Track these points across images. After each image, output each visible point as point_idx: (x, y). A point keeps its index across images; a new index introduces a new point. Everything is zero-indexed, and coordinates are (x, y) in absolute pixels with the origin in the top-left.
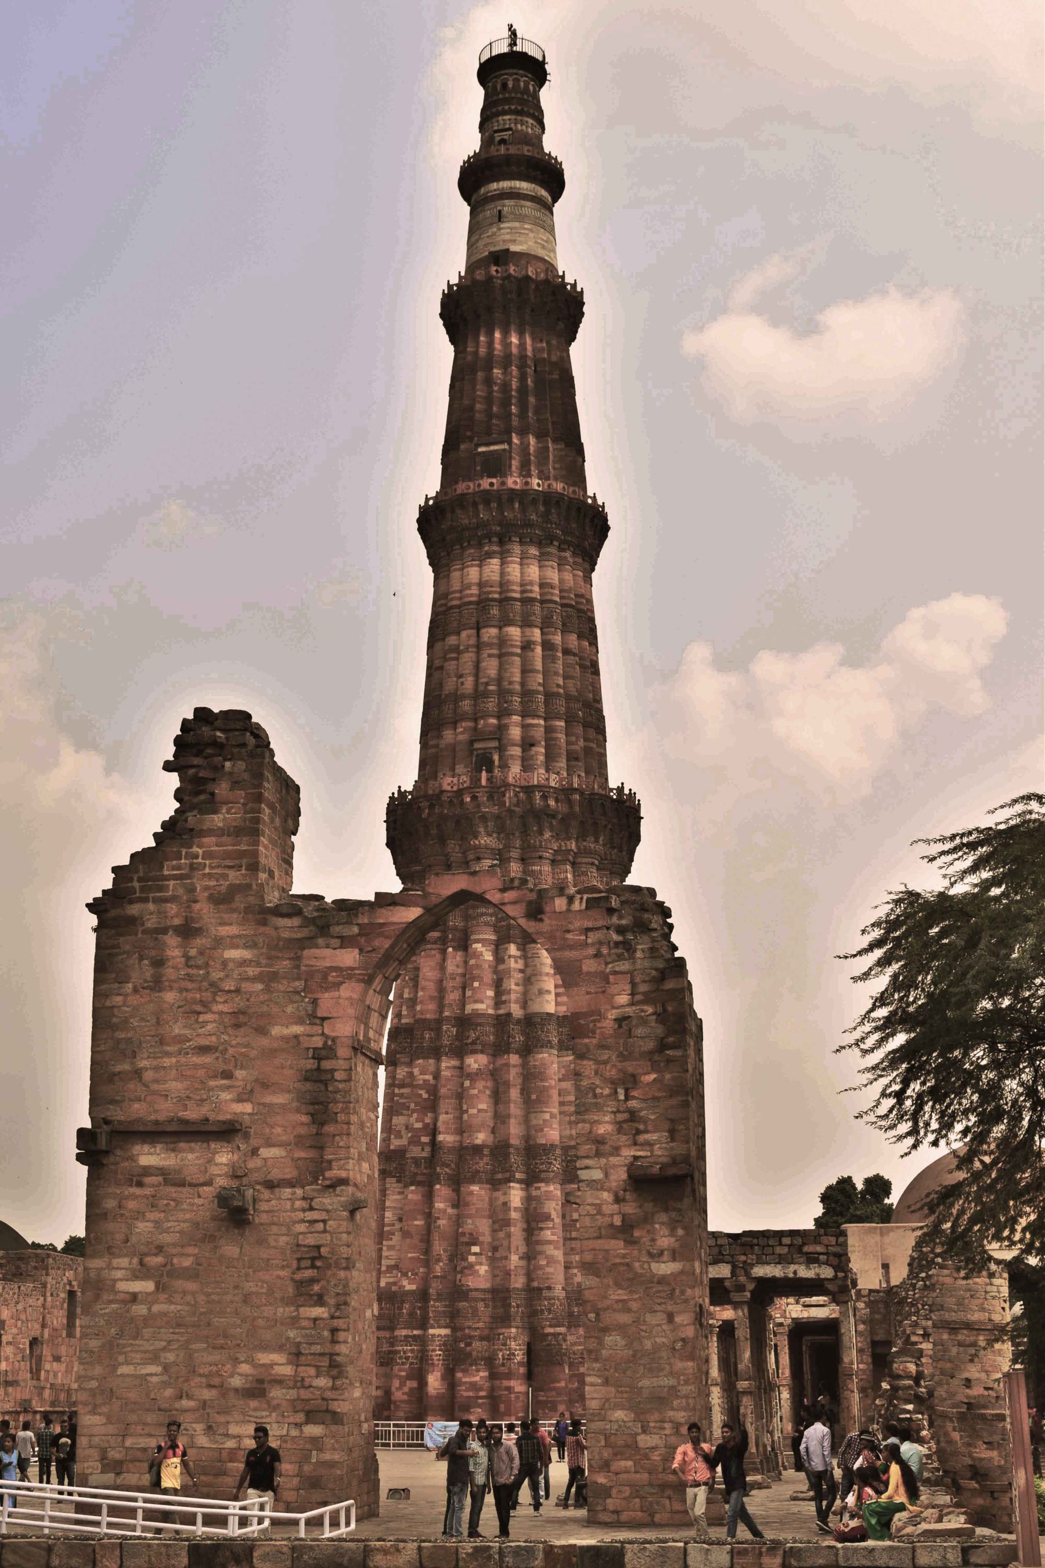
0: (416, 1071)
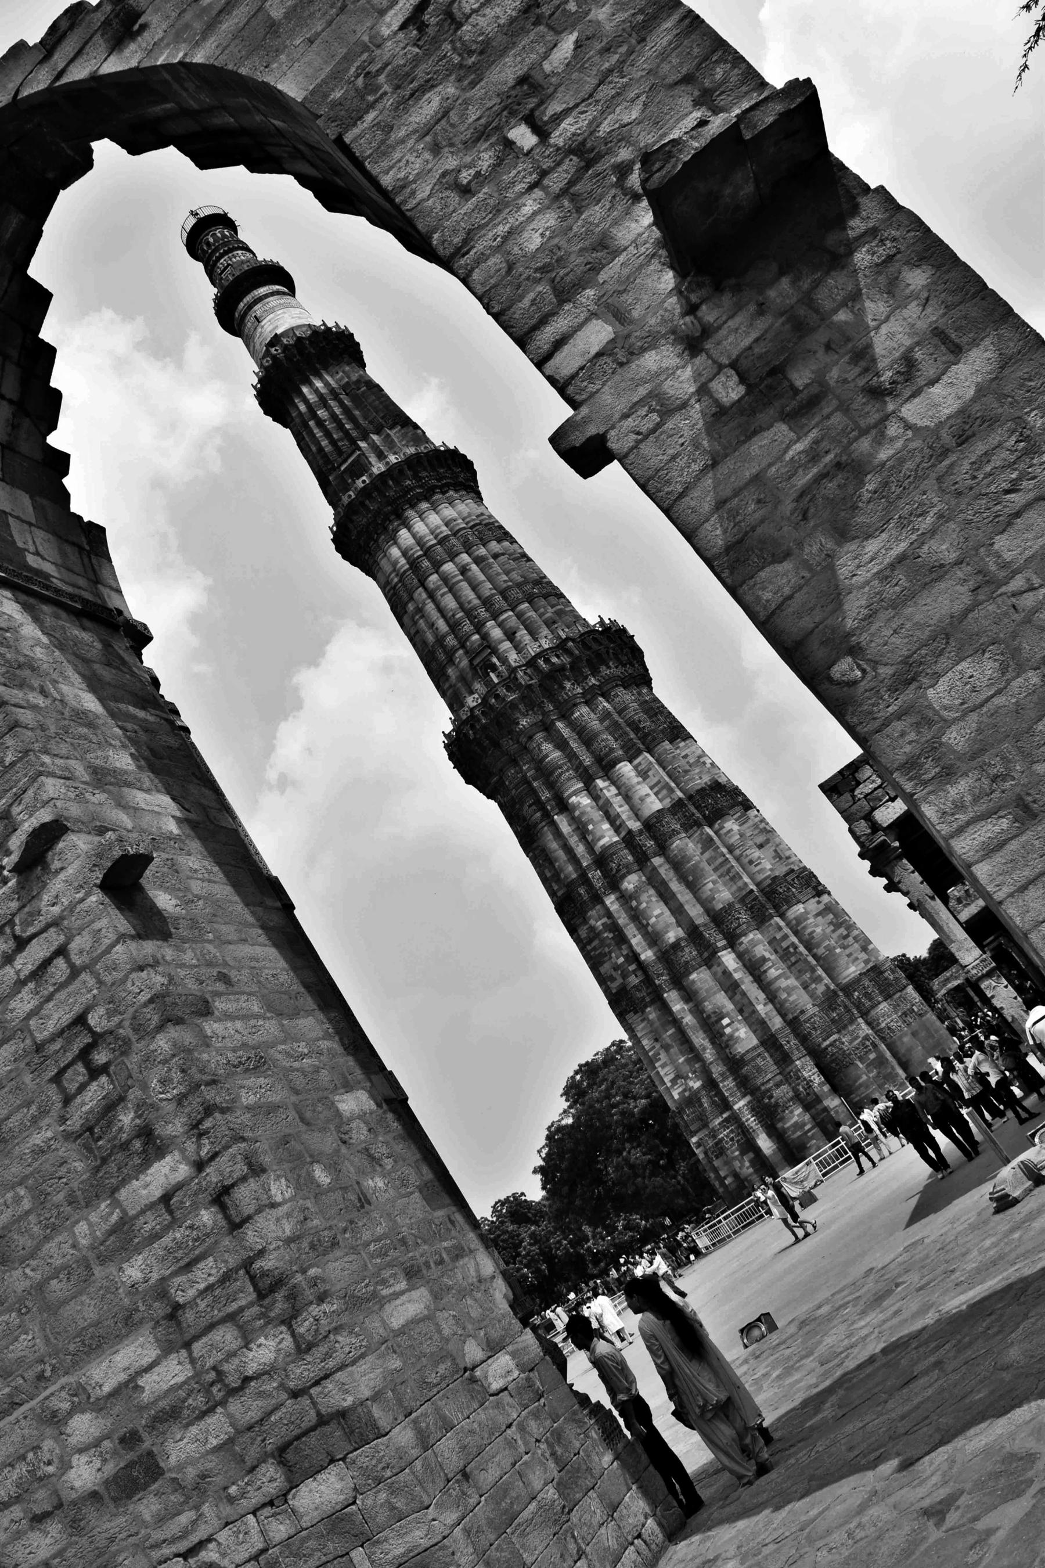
0: (592, 922)
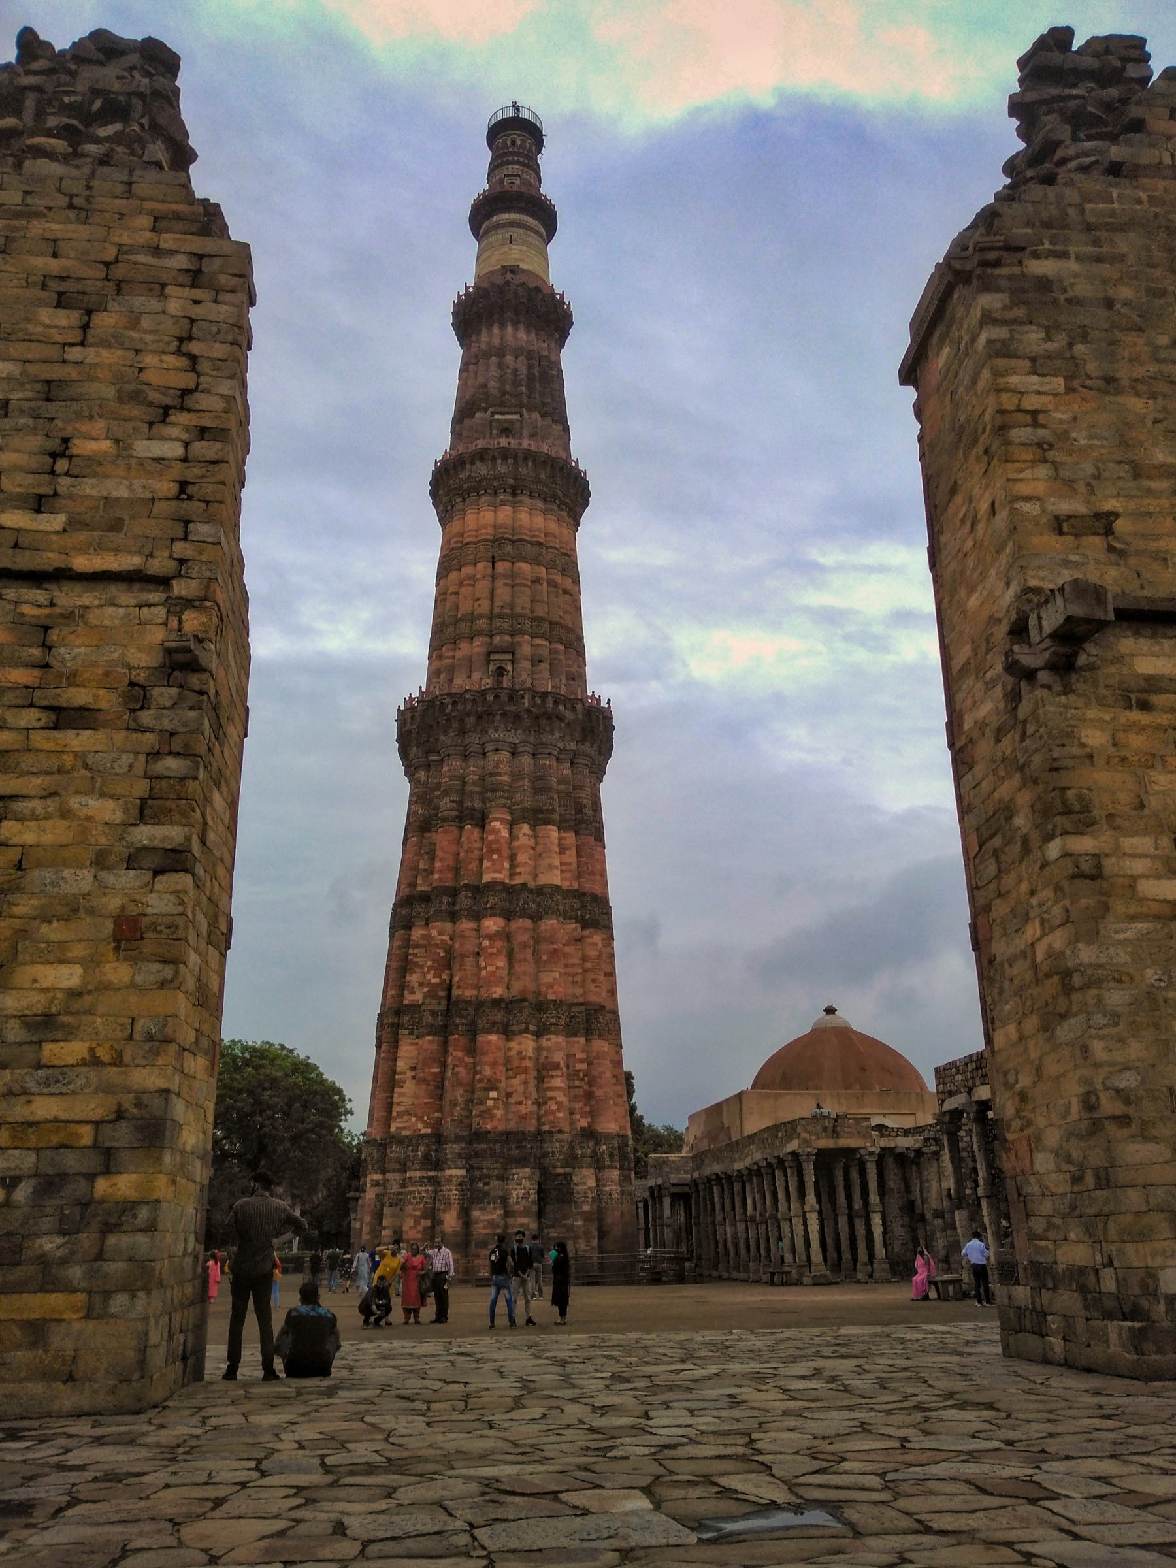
0: (434, 932)
